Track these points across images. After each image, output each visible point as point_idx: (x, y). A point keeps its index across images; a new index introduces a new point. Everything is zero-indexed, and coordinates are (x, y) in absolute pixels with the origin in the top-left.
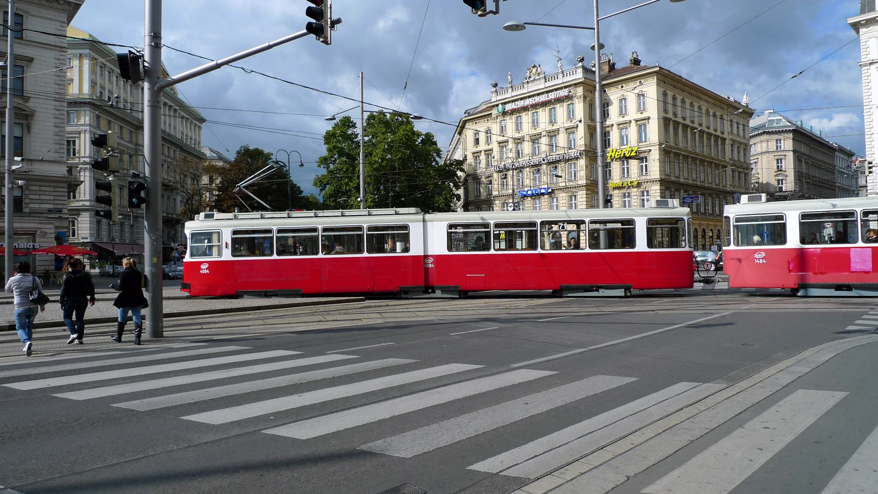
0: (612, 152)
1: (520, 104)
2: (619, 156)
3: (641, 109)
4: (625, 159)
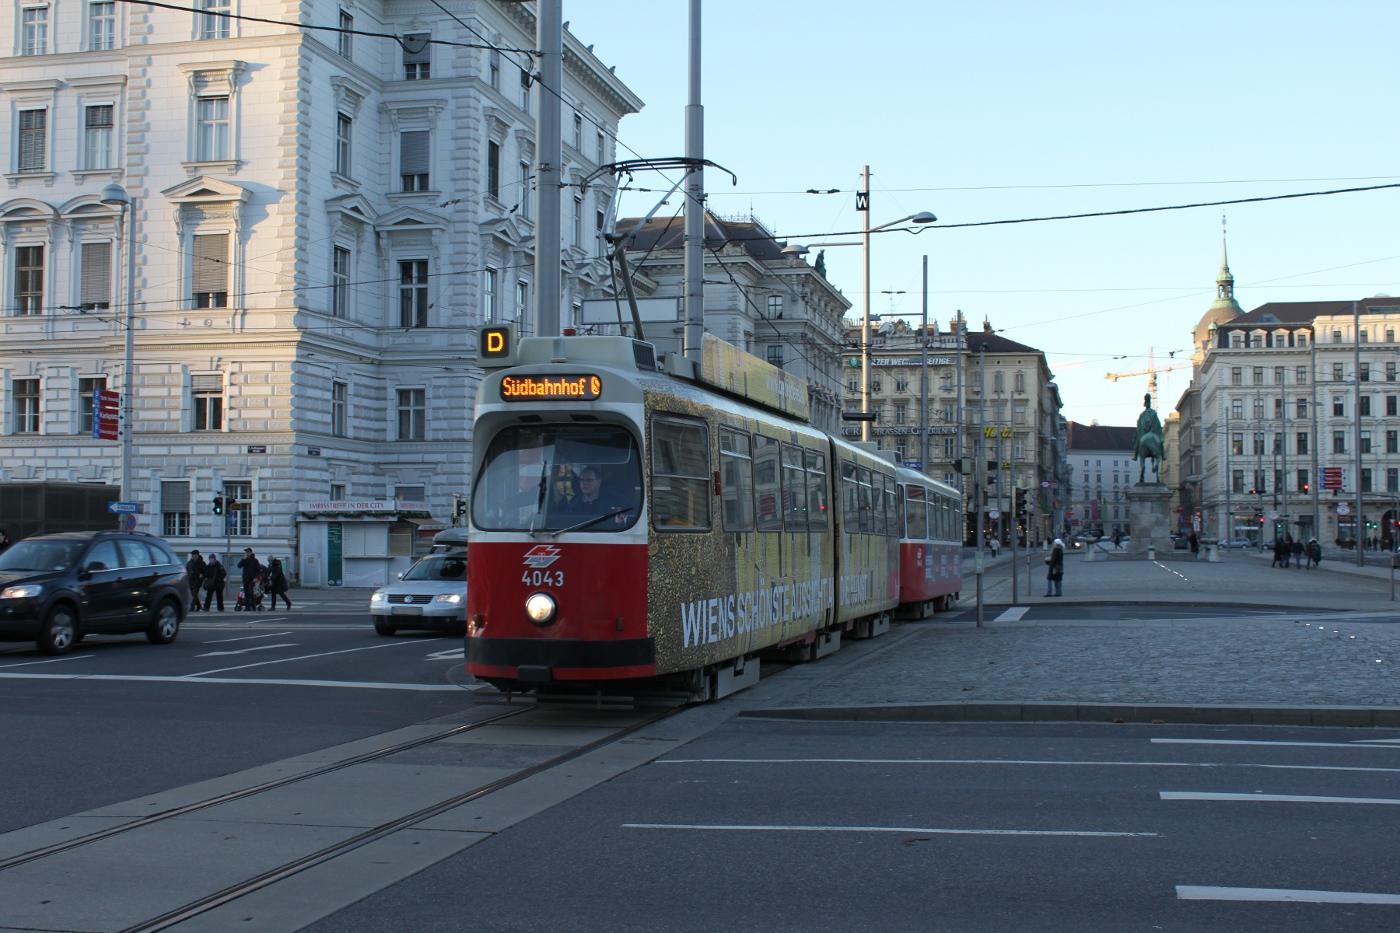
1: (886, 361)
4: (999, 440)
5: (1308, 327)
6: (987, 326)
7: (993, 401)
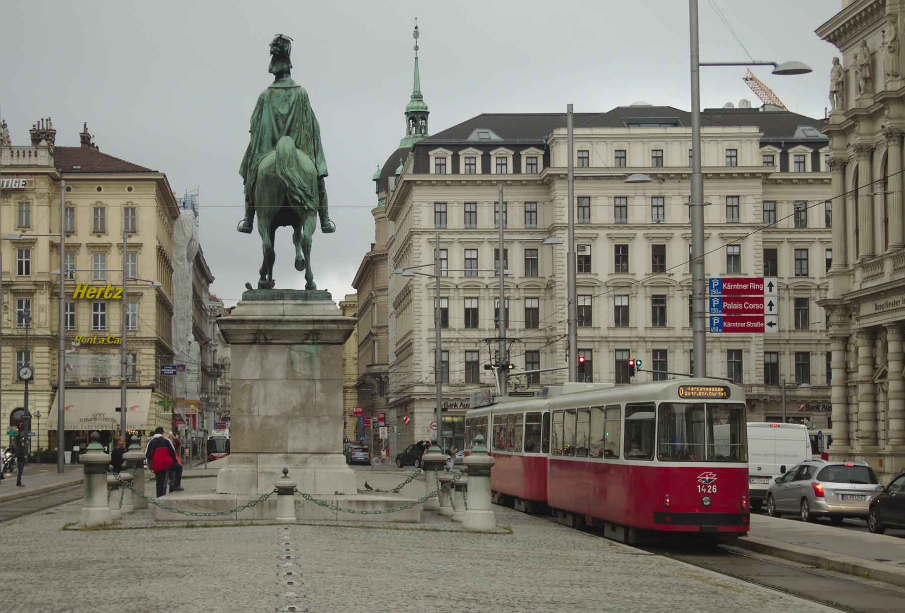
0: (82, 288)
2: (93, 296)
3: (130, 229)
4: (99, 304)
5: (540, 146)
6: (85, 138)
7: (90, 246)
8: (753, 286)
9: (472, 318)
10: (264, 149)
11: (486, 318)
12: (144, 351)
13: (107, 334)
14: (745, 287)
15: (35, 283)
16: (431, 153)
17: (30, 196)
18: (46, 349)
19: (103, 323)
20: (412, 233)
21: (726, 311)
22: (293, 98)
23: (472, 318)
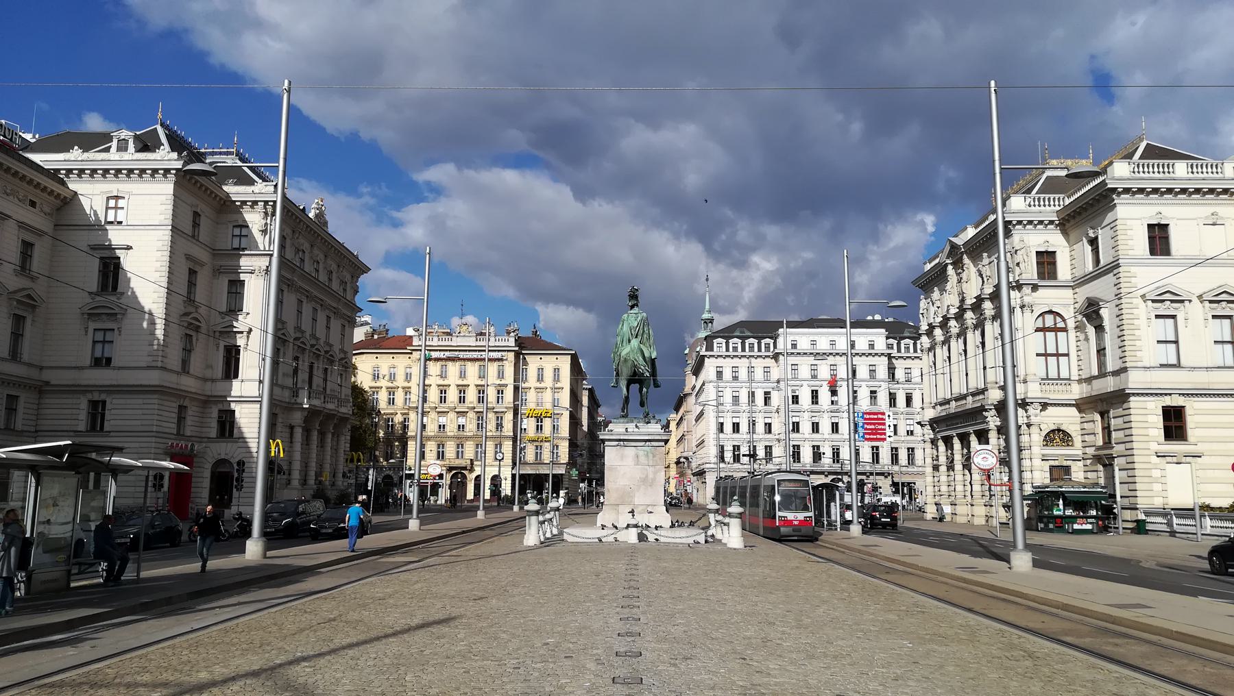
8: (880, 416)
9: (736, 427)
10: (624, 344)
11: (744, 427)
12: (562, 444)
13: (543, 435)
14: (876, 417)
15: (506, 408)
16: (714, 341)
17: (504, 362)
18: (511, 443)
19: (541, 430)
20: (703, 384)
21: (866, 429)
22: (639, 318)
23: (736, 427)
